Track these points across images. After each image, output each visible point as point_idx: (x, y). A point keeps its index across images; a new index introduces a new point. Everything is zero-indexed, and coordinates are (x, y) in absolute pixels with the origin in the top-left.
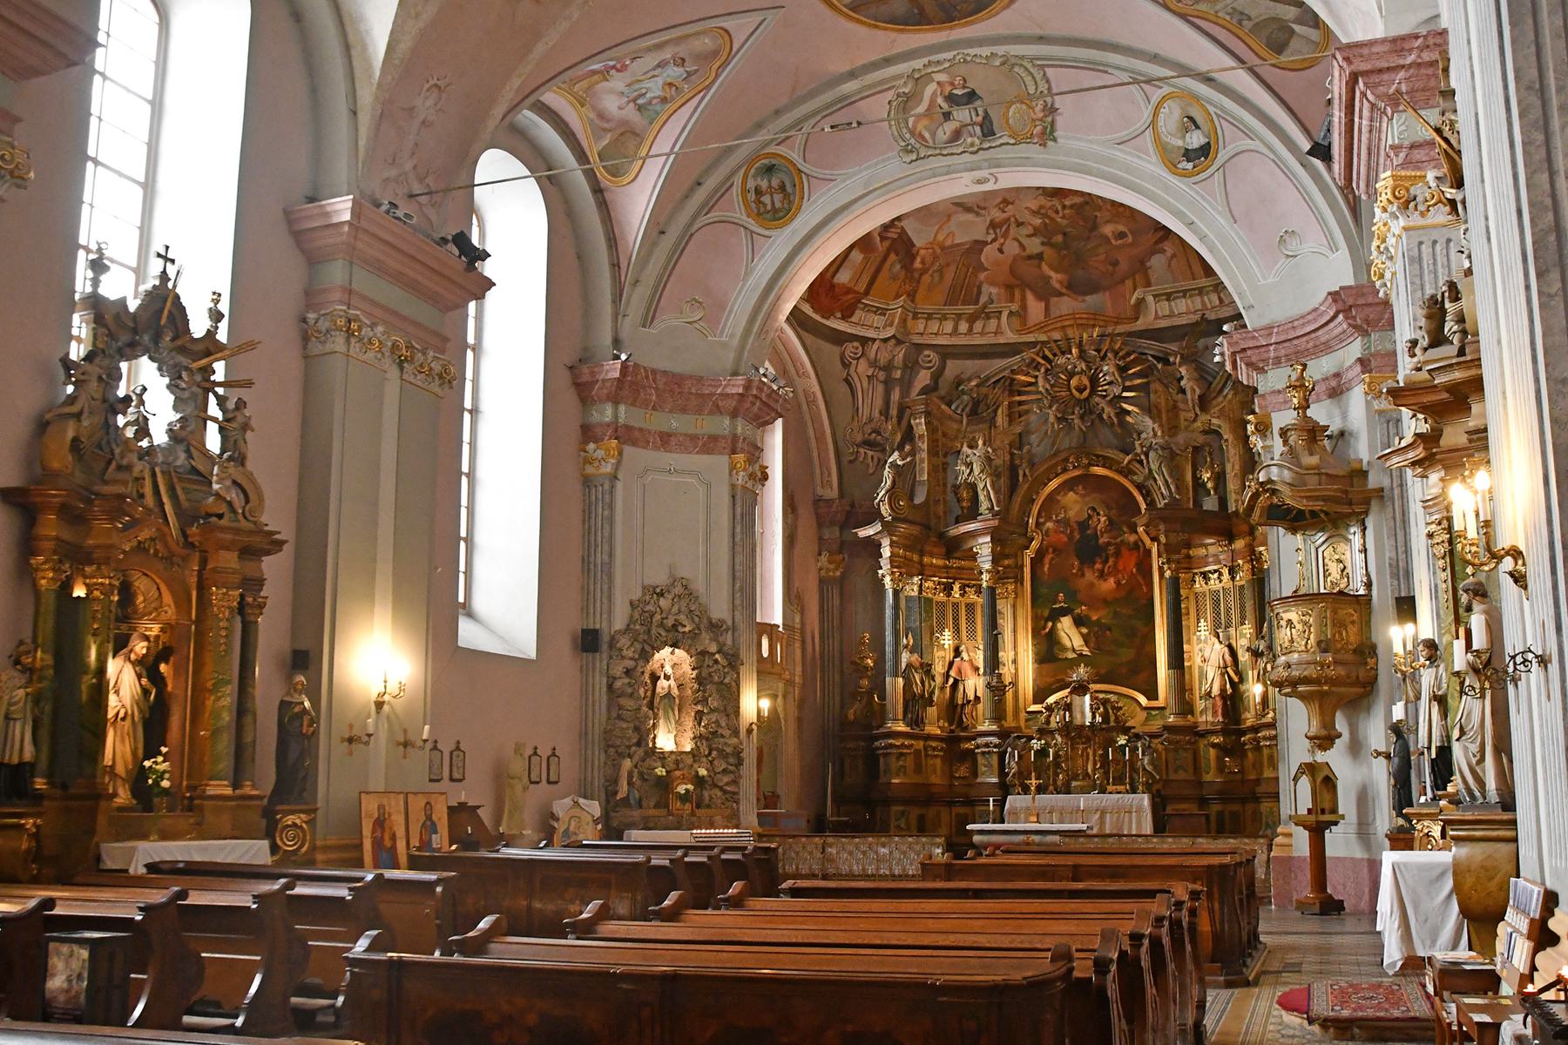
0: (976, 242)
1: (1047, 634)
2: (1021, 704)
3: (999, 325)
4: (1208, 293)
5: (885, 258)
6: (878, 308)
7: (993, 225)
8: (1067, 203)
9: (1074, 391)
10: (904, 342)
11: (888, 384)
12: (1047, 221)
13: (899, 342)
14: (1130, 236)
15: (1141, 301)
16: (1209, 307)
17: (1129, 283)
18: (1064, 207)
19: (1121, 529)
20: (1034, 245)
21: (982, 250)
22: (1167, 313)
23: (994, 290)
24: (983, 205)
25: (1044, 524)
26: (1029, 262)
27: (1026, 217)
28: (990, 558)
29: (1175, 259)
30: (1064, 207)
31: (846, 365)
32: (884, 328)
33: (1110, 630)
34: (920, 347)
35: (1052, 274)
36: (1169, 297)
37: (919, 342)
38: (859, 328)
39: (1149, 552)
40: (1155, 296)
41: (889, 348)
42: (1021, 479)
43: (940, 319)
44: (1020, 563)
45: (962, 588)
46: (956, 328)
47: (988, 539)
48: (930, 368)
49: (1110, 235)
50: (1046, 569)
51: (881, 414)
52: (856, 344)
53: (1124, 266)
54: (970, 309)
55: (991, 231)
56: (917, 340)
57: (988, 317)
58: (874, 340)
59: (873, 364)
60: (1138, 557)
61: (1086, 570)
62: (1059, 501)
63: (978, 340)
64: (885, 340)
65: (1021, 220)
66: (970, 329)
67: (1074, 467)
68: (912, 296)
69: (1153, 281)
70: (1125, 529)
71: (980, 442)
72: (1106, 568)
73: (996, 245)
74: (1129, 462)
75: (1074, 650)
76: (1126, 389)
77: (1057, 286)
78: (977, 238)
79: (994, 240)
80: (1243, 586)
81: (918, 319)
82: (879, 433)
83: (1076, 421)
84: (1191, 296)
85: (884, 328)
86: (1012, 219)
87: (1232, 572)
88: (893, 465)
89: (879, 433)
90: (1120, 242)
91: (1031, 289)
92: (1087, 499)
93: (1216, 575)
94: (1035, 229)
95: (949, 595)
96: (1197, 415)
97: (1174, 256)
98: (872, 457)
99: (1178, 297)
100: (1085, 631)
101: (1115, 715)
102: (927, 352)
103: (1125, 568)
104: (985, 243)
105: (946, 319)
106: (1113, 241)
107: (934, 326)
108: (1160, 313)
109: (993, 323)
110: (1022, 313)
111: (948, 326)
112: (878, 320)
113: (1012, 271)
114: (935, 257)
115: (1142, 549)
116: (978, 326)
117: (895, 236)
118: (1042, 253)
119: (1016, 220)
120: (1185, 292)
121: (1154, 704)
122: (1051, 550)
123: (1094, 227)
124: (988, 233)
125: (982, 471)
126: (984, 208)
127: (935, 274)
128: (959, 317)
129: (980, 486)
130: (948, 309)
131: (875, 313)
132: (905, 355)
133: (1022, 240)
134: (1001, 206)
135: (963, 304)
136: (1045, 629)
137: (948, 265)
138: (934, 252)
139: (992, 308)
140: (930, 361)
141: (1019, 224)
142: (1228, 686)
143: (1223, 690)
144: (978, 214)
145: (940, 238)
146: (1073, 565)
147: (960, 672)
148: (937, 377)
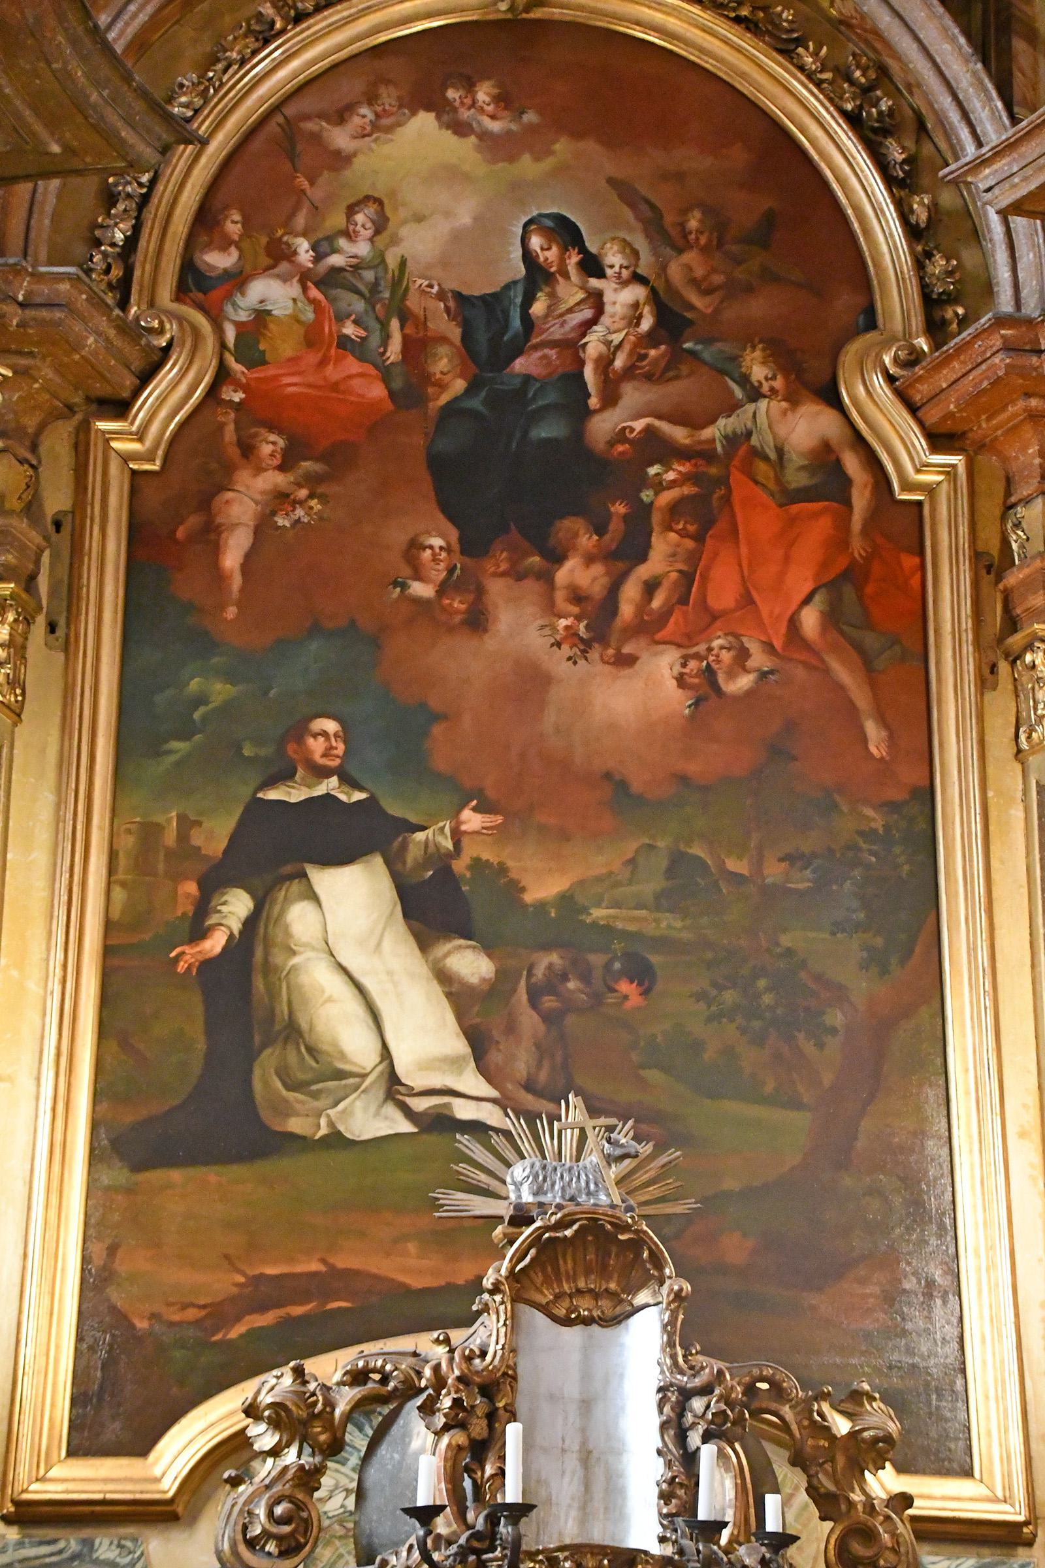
1: (208, 965)
19: (729, 368)
25: (238, 280)
33: (642, 974)
44: (57, 500)
50: (232, 559)
60: (840, 540)
61: (496, 588)
62: (341, 160)
70: (759, 373)
72: (631, 592)
92: (528, 167)
103: (747, 601)
115: (860, 499)
122: (270, 445)
136: (199, 932)
146: (415, 546)
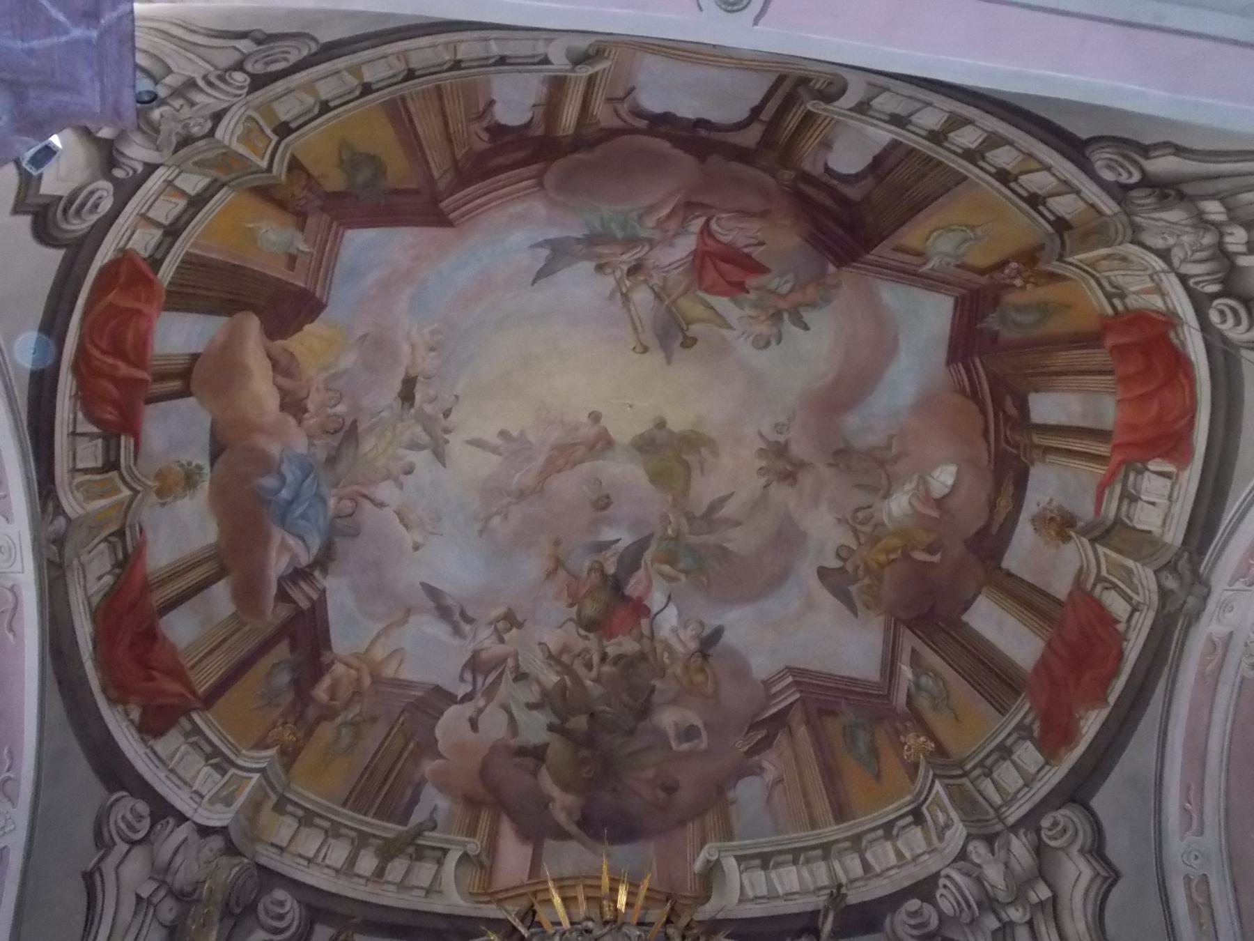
0: (438, 691)
3: (436, 878)
4: (841, 852)
5: (265, 647)
6: (217, 752)
7: (475, 665)
8: (611, 650)
10: (241, 854)
12: (569, 683)
13: (231, 850)
16: (844, 880)
17: (692, 828)
18: (604, 657)
20: (535, 728)
21: (442, 713)
22: (765, 892)
23: (443, 803)
24: (470, 613)
26: (517, 760)
27: (535, 664)
29: (780, 786)
31: (102, 841)
32: (212, 801)
34: (269, 877)
35: (555, 792)
36: (765, 861)
38: (162, 774)
40: (739, 859)
41: (206, 853)
43: (326, 832)
46: (352, 860)
49: (671, 732)
52: (142, 807)
53: (685, 796)
54: (392, 829)
55: (468, 677)
56: (269, 858)
57: (420, 854)
58: (182, 818)
59: (161, 873)
64: (205, 831)
65: (524, 668)
68: (289, 756)
69: (737, 828)
73: (468, 709)
77: (562, 818)
78: (440, 682)
79: (468, 697)
84: (808, 861)
85: (212, 801)
86: (510, 662)
90: (685, 746)
91: (513, 819)
94: (545, 694)
97: (779, 781)
102: (280, 894)
104: (451, 699)
105: (337, 836)
106: (674, 744)
107: (310, 843)
108: (751, 894)
109: (424, 873)
110: (486, 862)
111: (338, 853)
112: (206, 778)
113: (484, 772)
114: (357, 693)
116: (397, 869)
117: (304, 604)
118: (545, 746)
119: (517, 666)
120: (796, 853)
123: (645, 711)
124: (462, 679)
126: (470, 621)
127: (344, 731)
128: (362, 840)
130: (348, 817)
131: (208, 757)
135: (376, 816)
137: (374, 719)
138: (359, 680)
139: (430, 839)
144: (457, 632)
145: (379, 653)
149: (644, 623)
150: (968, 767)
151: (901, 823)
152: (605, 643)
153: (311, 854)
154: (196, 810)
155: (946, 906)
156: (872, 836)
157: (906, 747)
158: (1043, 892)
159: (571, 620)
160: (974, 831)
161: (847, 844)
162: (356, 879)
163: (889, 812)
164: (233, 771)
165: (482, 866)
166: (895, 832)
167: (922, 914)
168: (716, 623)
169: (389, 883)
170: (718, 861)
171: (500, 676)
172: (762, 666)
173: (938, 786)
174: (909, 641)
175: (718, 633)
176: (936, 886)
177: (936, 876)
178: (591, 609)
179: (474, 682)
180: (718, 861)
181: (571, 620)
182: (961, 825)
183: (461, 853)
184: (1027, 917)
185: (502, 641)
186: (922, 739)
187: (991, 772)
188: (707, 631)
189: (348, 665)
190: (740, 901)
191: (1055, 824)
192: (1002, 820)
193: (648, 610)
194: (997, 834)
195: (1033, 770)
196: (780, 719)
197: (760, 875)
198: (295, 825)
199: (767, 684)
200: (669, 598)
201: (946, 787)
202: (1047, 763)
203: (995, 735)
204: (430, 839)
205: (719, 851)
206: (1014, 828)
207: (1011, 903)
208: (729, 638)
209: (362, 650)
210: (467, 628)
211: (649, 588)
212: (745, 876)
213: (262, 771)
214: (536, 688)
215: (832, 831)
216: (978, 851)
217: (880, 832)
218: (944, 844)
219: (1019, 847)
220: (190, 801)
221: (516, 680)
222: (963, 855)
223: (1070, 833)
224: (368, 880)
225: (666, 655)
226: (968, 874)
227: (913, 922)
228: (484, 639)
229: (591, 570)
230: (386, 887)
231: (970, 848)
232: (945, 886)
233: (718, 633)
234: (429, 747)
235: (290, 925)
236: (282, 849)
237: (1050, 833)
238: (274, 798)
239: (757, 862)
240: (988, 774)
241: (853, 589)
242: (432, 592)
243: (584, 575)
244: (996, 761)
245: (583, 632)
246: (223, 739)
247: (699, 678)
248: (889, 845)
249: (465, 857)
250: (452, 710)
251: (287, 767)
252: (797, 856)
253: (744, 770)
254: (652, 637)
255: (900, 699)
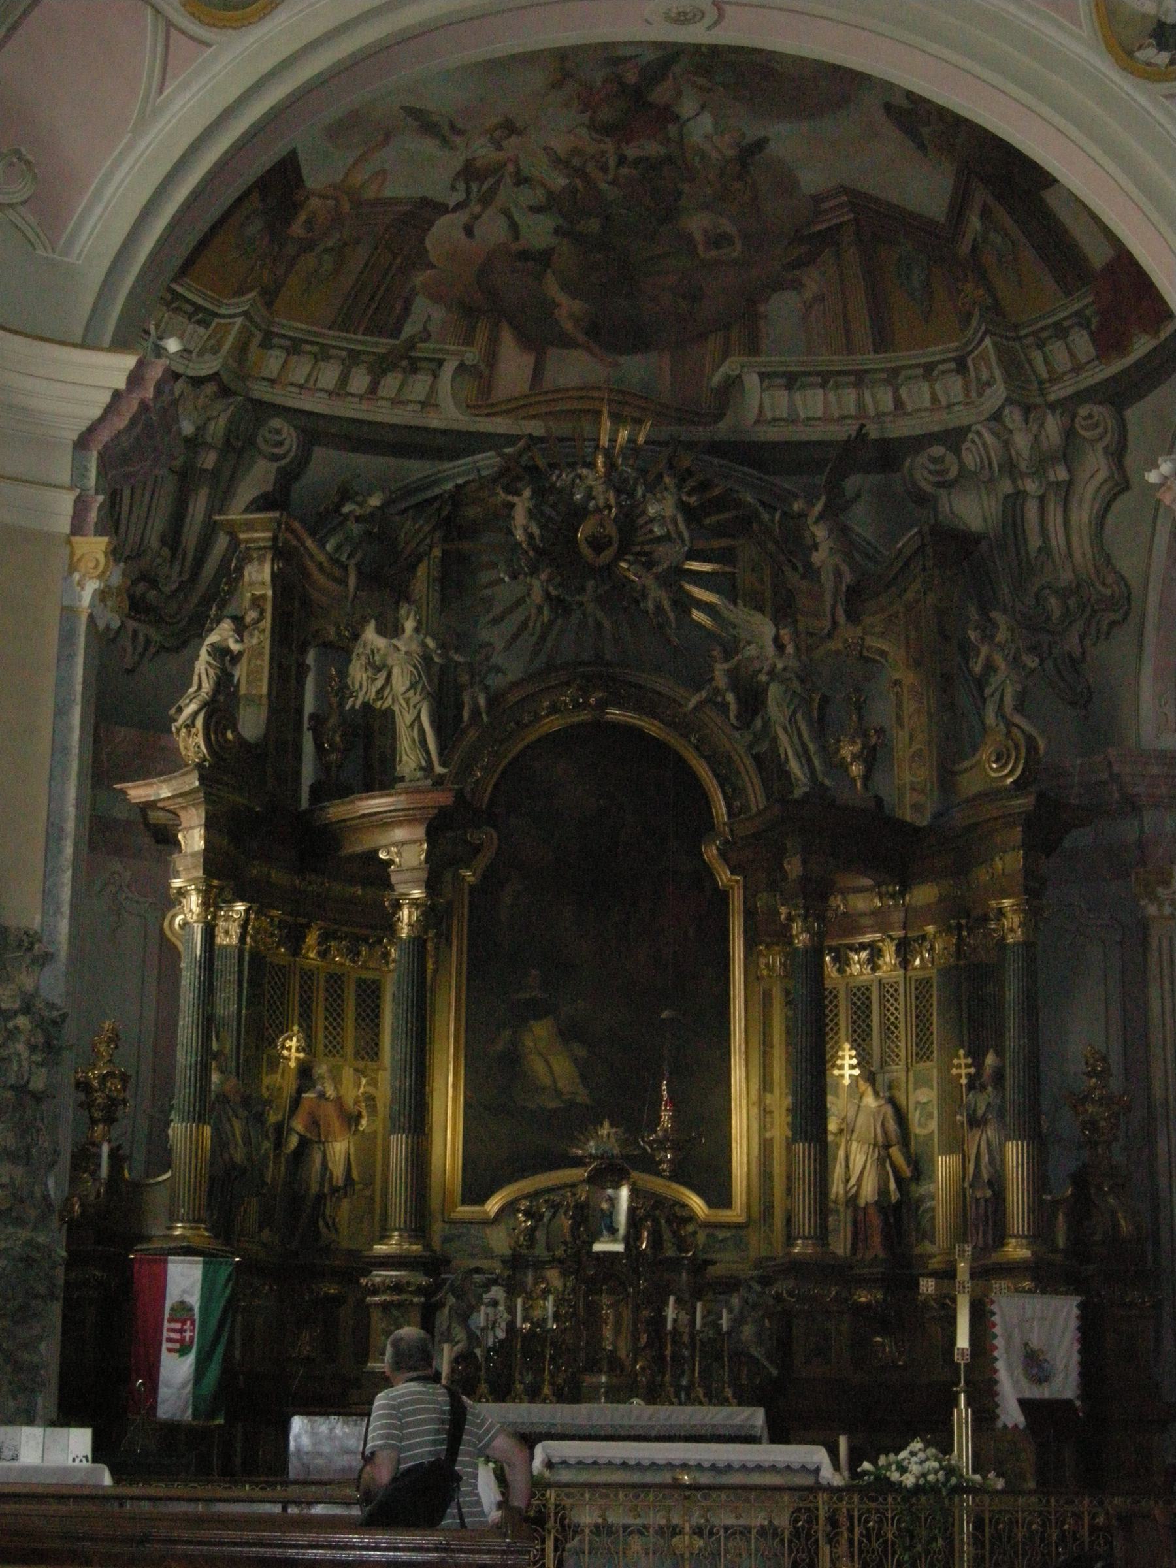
0: (425, 202)
2: (435, 1203)
3: (433, 389)
6: (198, 308)
7: (469, 172)
8: (631, 152)
9: (586, 550)
10: (235, 394)
11: (187, 478)
13: (225, 392)
14: (738, 245)
15: (733, 384)
16: (872, 412)
18: (622, 160)
21: (431, 223)
23: (438, 314)
24: (459, 126)
27: (539, 168)
28: (424, 875)
30: (622, 160)
34: (262, 410)
35: (562, 298)
36: (792, 381)
37: (267, 398)
39: (723, 897)
40: (762, 376)
41: (202, 401)
42: (466, 715)
43: (315, 357)
45: (325, 938)
46: (344, 379)
47: (420, 832)
48: (275, 458)
49: (699, 237)
51: (163, 541)
54: (382, 345)
55: (461, 186)
63: (384, 414)
64: (197, 382)
65: (526, 173)
66: (373, 389)
67: (577, 705)
68: (270, 296)
71: (409, 625)
73: (462, 217)
74: (696, 708)
75: (558, 1093)
76: (693, 555)
77: (568, 326)
78: (430, 194)
80: (928, 981)
81: (272, 347)
82: (153, 583)
83: (590, 607)
84: (837, 386)
85: (201, 354)
86: (510, 168)
87: (904, 950)
88: (220, 653)
89: (153, 583)
90: (714, 253)
93: (864, 955)
94: (550, 194)
95: (296, 951)
96: (835, 623)
97: (819, 298)
98: (135, 633)
99: (812, 386)
100: (582, 1052)
101: (675, 1233)
102: (276, 423)
104: (441, 209)
105: (327, 358)
106: (701, 249)
107: (300, 370)
108: (769, 415)
109: (419, 386)
110: (486, 373)
111: (329, 376)
116: (391, 383)
119: (518, 172)
121: (725, 1215)
124: (453, 188)
125: (413, 686)
127: (326, 257)
128: (354, 357)
129: (403, 719)
130: (333, 337)
132: (230, 421)
133: (517, 216)
134: (497, 133)
137: (357, 242)
139: (424, 350)
140: (280, 444)
141: (521, 180)
142: (893, 1185)
143: (883, 1191)
144: (445, 141)
145: (358, 179)
147: (315, 1123)
148: (288, 477)
149: (672, 130)
150: (1023, 332)
151: (941, 367)
152: (623, 145)
153: (302, 381)
154: (187, 366)
155: (969, 459)
156: (910, 372)
157: (962, 295)
158: (1062, 474)
159: (582, 124)
160: (1015, 396)
161: (884, 376)
162: (350, 399)
163: (934, 352)
164: (216, 320)
165: (480, 375)
166: (935, 373)
167: (943, 462)
168: (762, 133)
169: (382, 398)
170: (739, 376)
171: (499, 181)
172: (811, 180)
173: (988, 341)
174: (981, 195)
175: (760, 144)
176: (965, 440)
177: (969, 427)
178: (605, 114)
179: (468, 190)
180: (739, 376)
181: (582, 124)
182: (1002, 386)
183: (457, 363)
184: (1040, 493)
185: (499, 148)
186: (981, 292)
187: (1044, 346)
188: (744, 143)
189: (325, 197)
190: (757, 422)
191: (1091, 416)
192: (1042, 392)
193: (678, 118)
194: (1036, 406)
195: (1083, 358)
196: (828, 238)
197: (782, 396)
198: (284, 355)
199: (817, 199)
200: (703, 107)
201: (995, 344)
202: (1098, 358)
203: (1053, 312)
204: (424, 350)
205: (742, 367)
206: (1052, 407)
207: (1029, 475)
208: (773, 149)
209: (339, 178)
210: (458, 140)
211: (680, 93)
212: (766, 396)
213: (245, 314)
214: (540, 192)
215: (869, 360)
216: (1013, 417)
217: (920, 371)
218: (982, 400)
219: (1053, 427)
220: (181, 360)
221: (517, 184)
222: (997, 417)
223: (1100, 430)
224: (361, 397)
225: (697, 159)
226: (997, 435)
227: (932, 467)
228: (483, 151)
229: (605, 82)
230: (380, 403)
231: (1007, 411)
232: (973, 442)
233: (760, 144)
234: (420, 259)
235: (291, 446)
236: (272, 382)
237: (1083, 423)
238: (259, 336)
239: (782, 381)
240: (1041, 345)
241: (925, 131)
242: (414, 113)
243: (599, 84)
244: (1050, 337)
245: (598, 137)
246: (205, 297)
247: (737, 185)
248: (925, 387)
249: (462, 368)
250: (443, 221)
251: (269, 305)
252: (825, 379)
253: (777, 285)
254: (681, 141)
255: (964, 249)
